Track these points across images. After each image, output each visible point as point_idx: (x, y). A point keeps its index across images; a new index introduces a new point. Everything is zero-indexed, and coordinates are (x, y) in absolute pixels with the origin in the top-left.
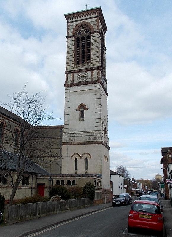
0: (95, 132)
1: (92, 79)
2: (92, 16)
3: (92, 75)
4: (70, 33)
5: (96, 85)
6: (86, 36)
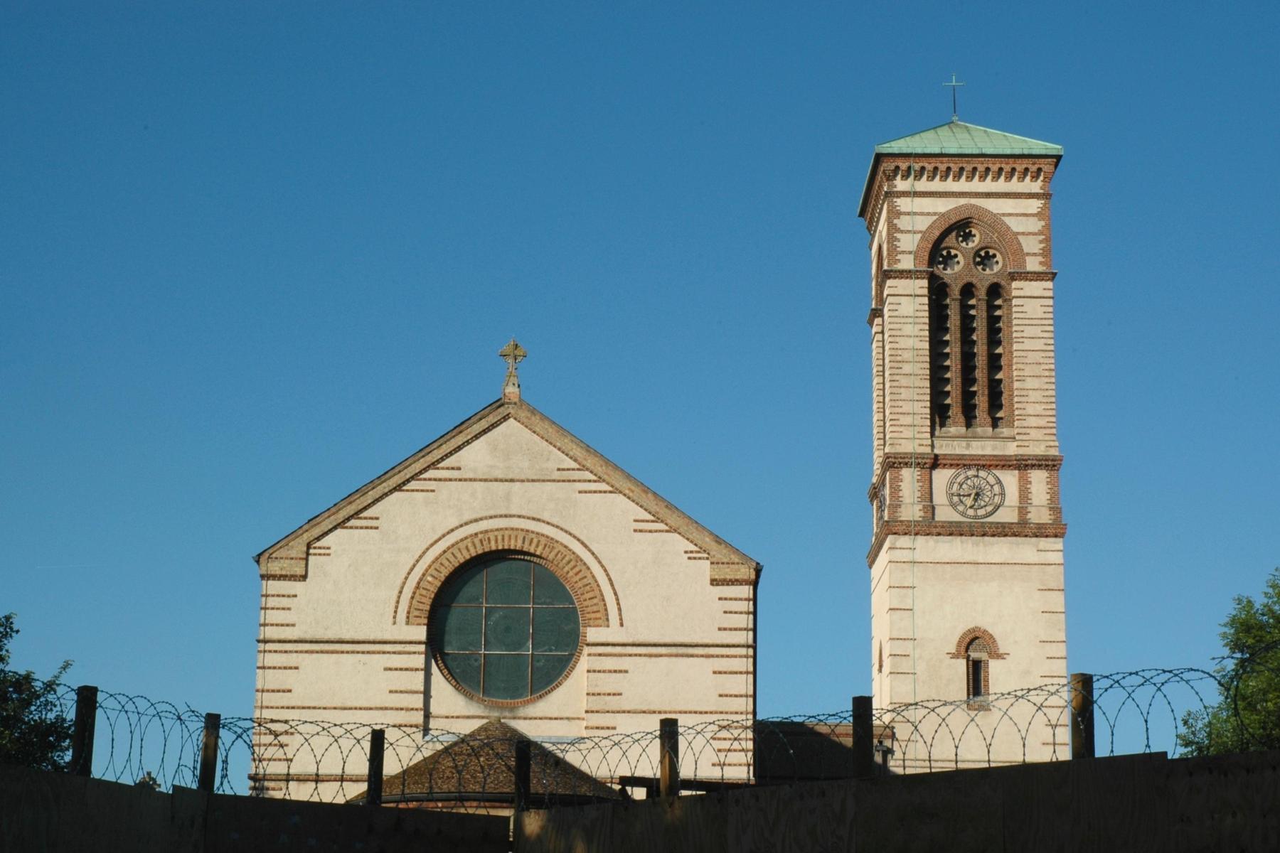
1: (1023, 510)
2: (1015, 185)
4: (903, 252)
5: (1044, 543)
6: (987, 284)
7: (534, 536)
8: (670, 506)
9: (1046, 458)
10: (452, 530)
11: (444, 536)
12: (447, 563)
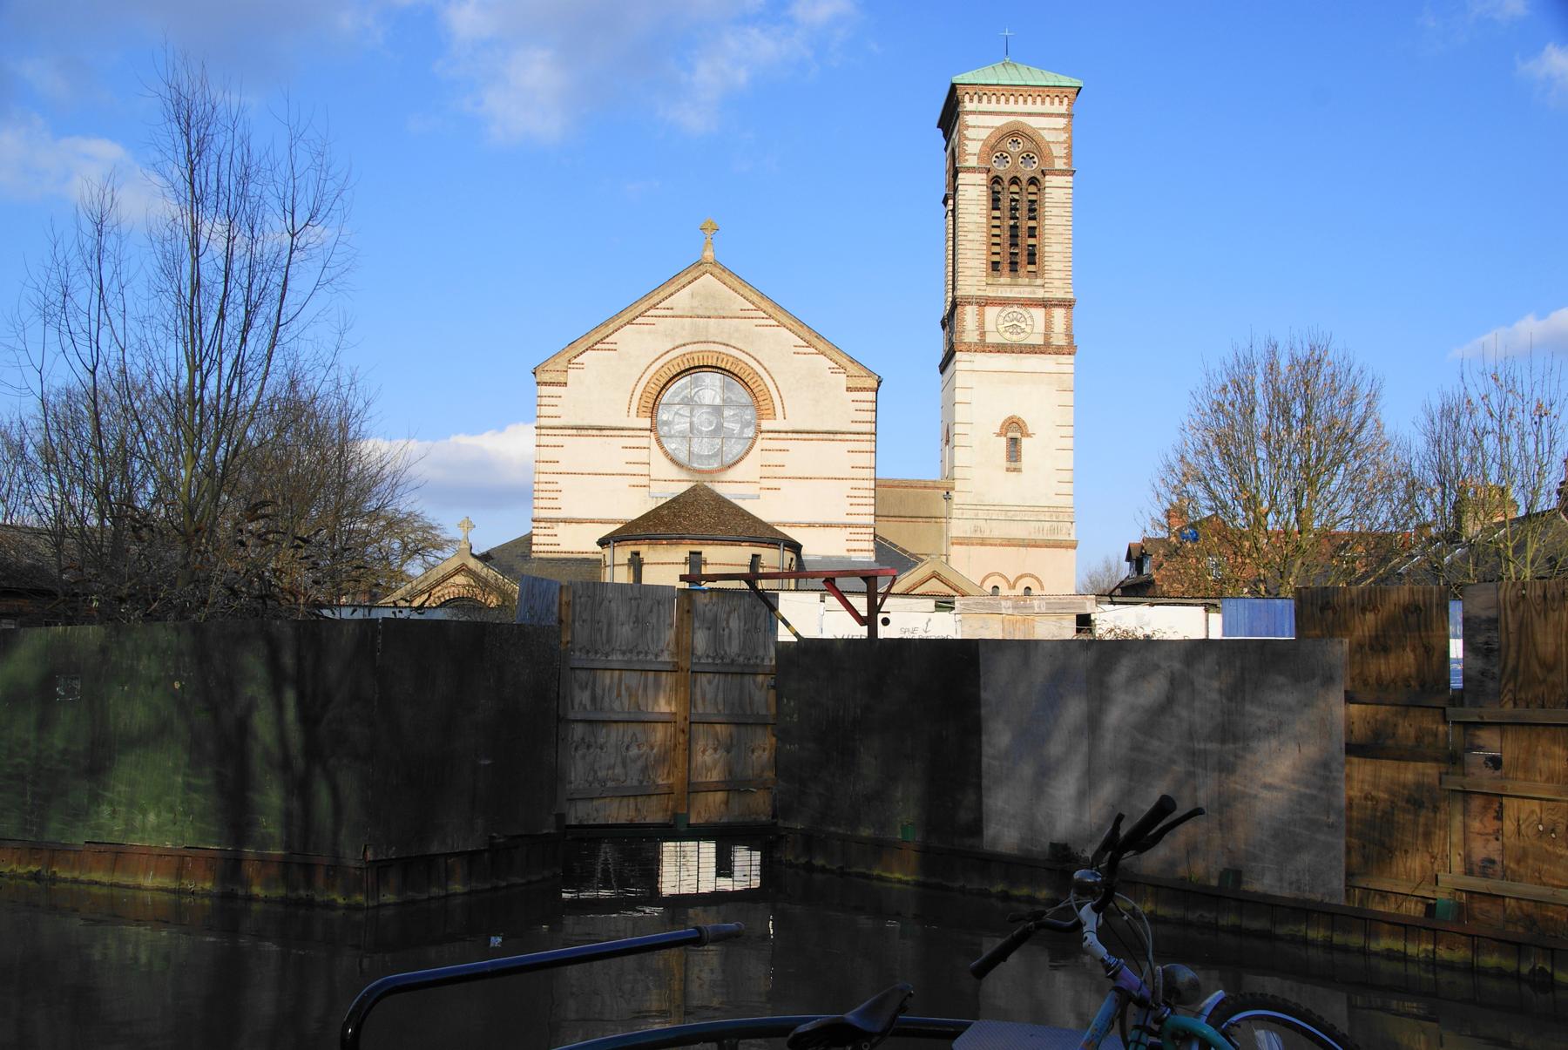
0: (1055, 510)
1: (1047, 336)
7: (724, 356)
8: (819, 336)
9: (1064, 300)
10: (668, 352)
11: (662, 355)
12: (664, 374)
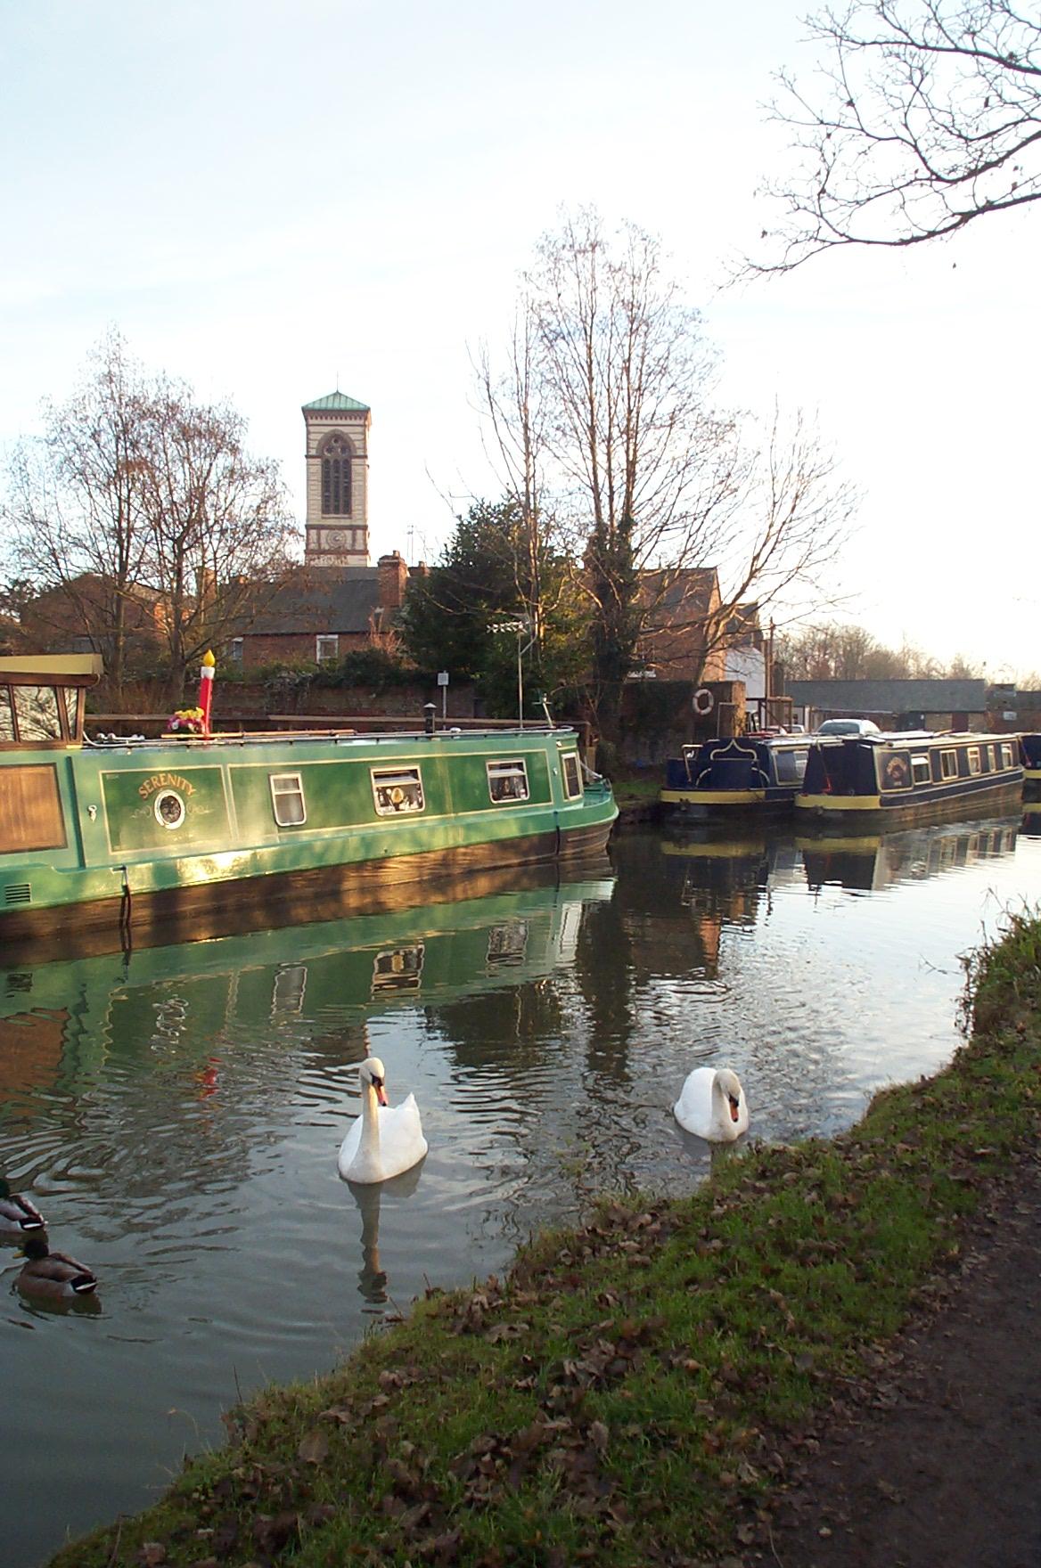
1: (353, 545)
2: (353, 422)
3: (354, 540)
